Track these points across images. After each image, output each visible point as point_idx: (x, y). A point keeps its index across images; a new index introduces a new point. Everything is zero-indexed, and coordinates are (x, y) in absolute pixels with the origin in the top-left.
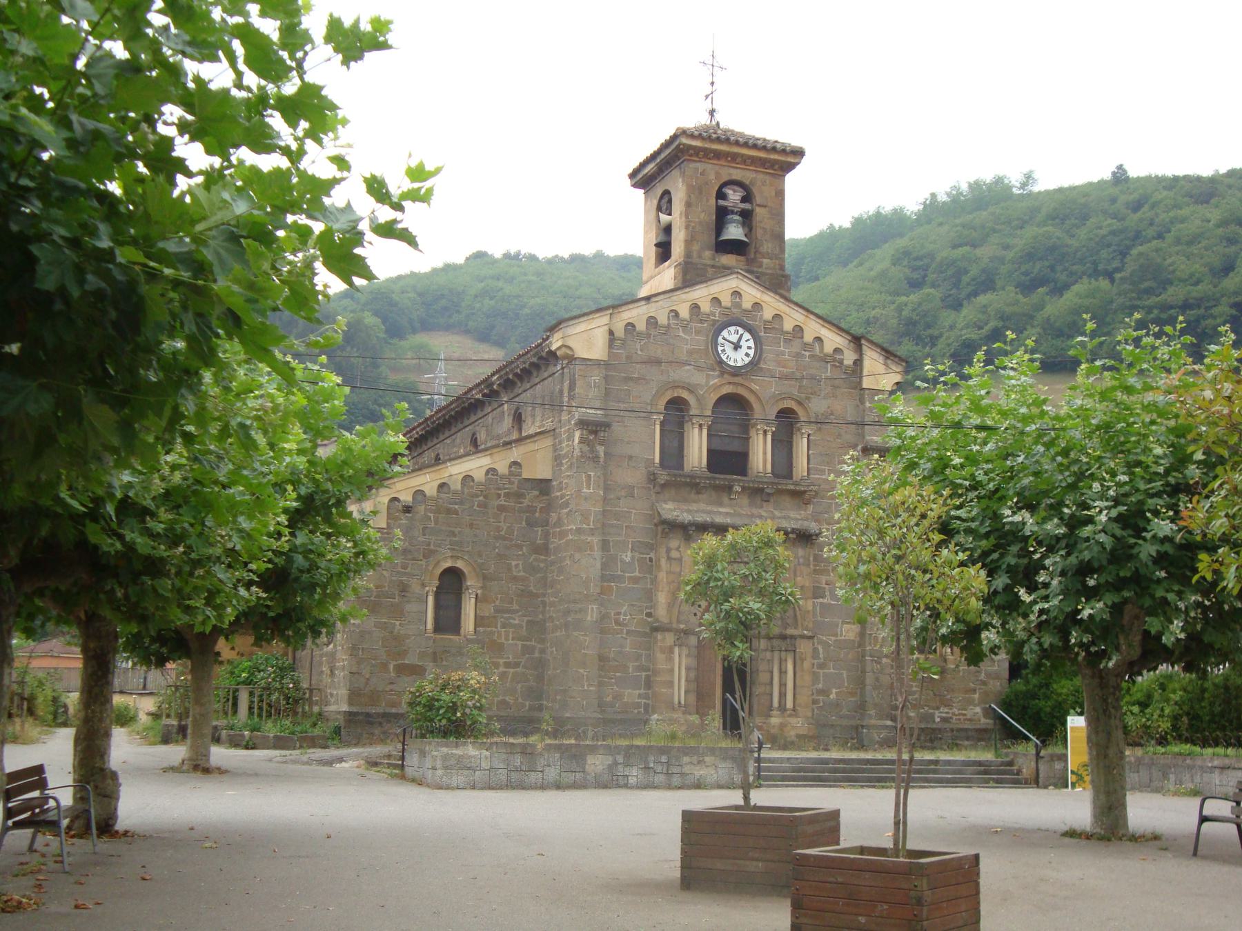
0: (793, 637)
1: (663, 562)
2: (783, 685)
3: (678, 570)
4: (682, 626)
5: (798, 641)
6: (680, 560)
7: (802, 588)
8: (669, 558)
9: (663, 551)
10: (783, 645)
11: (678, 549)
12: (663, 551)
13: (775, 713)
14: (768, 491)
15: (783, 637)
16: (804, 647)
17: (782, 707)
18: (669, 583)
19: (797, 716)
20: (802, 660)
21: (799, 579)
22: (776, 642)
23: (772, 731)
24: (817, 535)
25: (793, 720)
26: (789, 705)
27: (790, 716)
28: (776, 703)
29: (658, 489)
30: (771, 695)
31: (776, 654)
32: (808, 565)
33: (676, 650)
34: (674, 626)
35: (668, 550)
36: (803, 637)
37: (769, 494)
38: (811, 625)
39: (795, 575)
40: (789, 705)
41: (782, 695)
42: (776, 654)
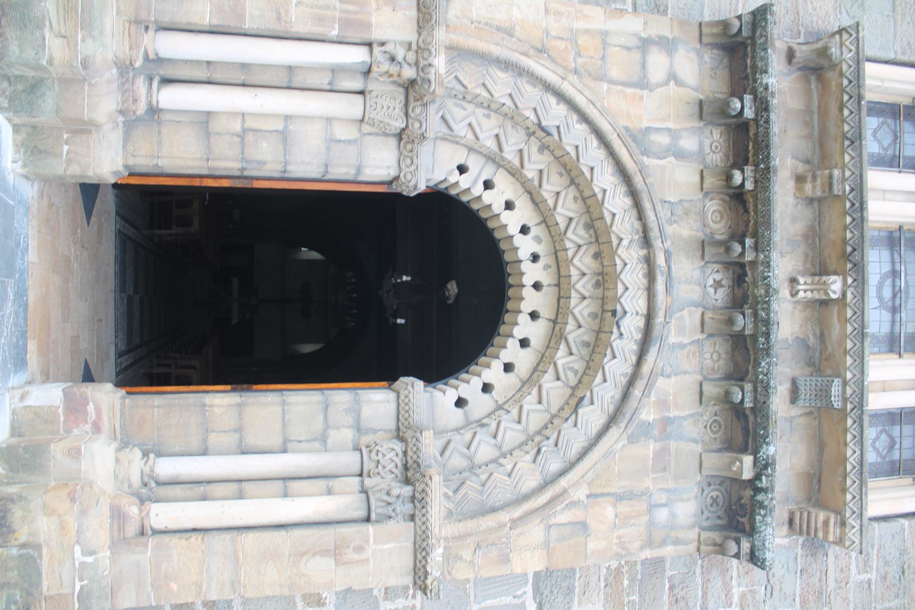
0: (418, 501)
1: (633, 25)
2: (240, 486)
3: (614, 73)
4: (440, 62)
5: (406, 529)
6: (642, 83)
7: (584, 525)
8: (645, 44)
9: (661, 27)
10: (385, 481)
11: (672, 77)
12: (661, 27)
13: (135, 464)
14: (836, 388)
15: (411, 472)
16: (384, 553)
17: (154, 489)
18: (572, 37)
19: (119, 542)
20: (337, 552)
21: (609, 511)
22: (391, 453)
23: (57, 450)
24: (754, 558)
25: (98, 529)
26: (164, 515)
27: (118, 515)
28: (167, 467)
29: (802, 52)
30: (205, 452)
31: (351, 460)
32: (649, 543)
33: (356, 56)
34: (441, 36)
35: (667, 45)
36: (421, 550)
37: (824, 393)
38: (461, 572)
39: (620, 498)
40: (164, 515)
41: (200, 488)
42: (351, 460)
